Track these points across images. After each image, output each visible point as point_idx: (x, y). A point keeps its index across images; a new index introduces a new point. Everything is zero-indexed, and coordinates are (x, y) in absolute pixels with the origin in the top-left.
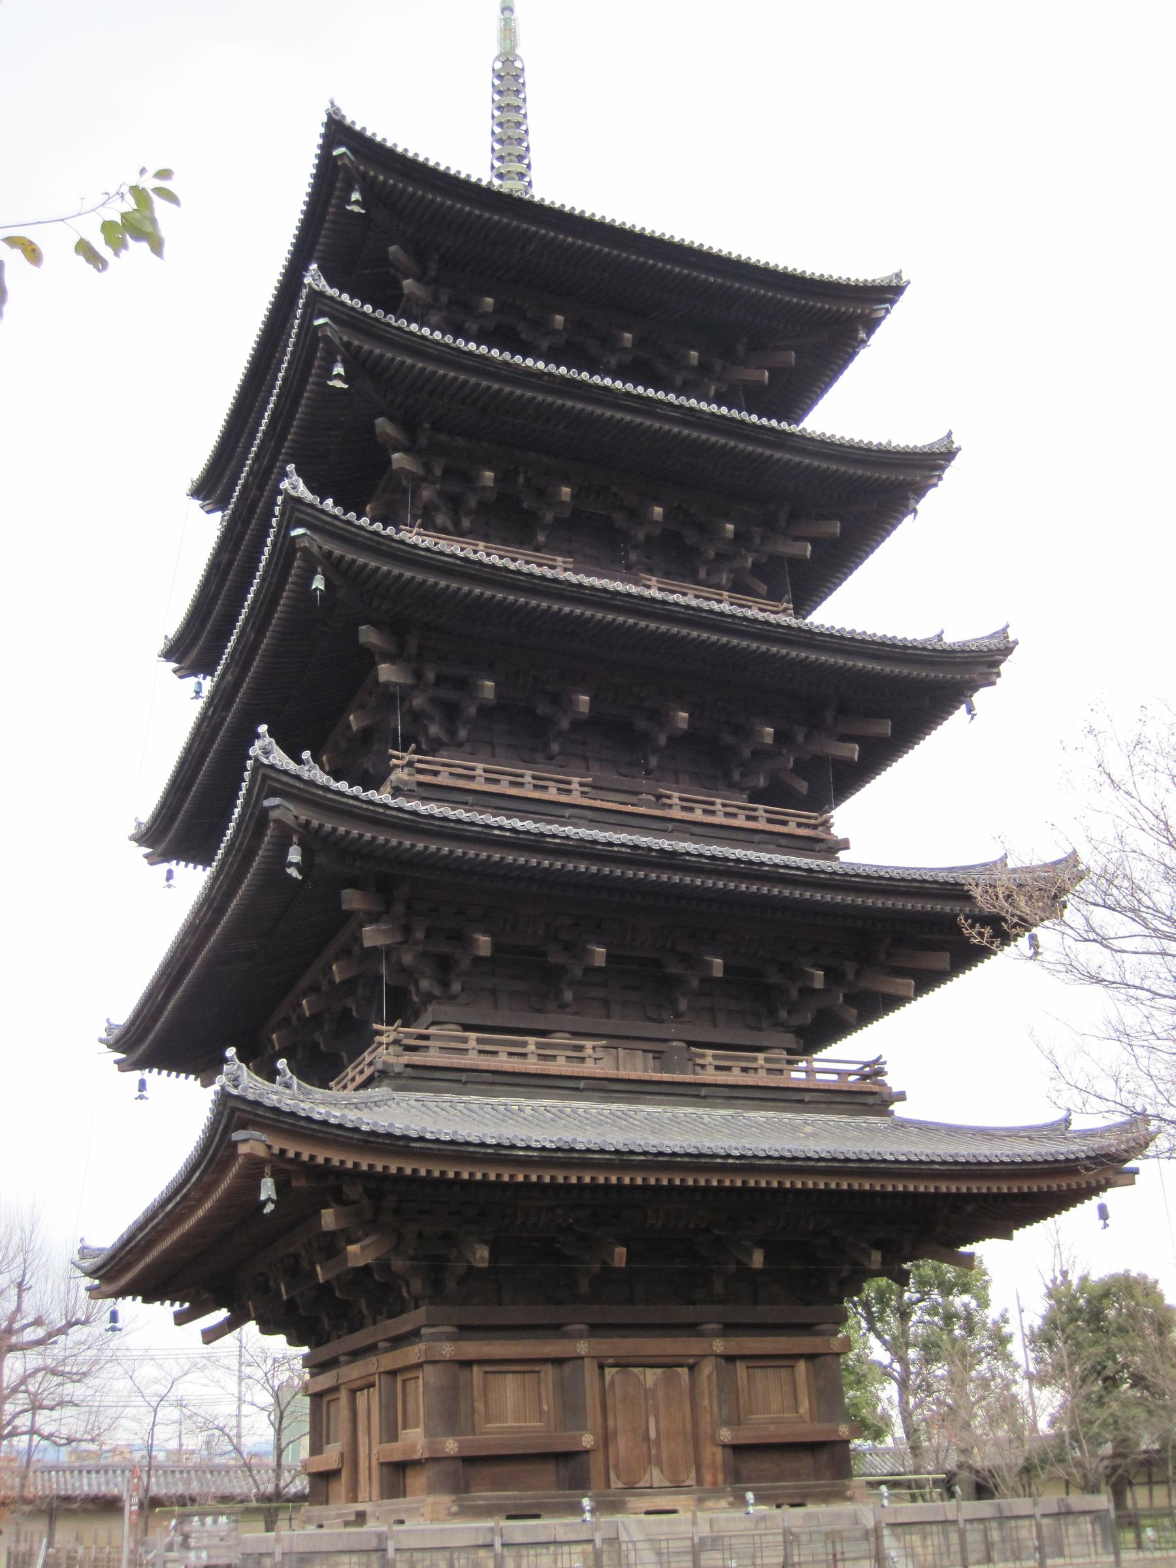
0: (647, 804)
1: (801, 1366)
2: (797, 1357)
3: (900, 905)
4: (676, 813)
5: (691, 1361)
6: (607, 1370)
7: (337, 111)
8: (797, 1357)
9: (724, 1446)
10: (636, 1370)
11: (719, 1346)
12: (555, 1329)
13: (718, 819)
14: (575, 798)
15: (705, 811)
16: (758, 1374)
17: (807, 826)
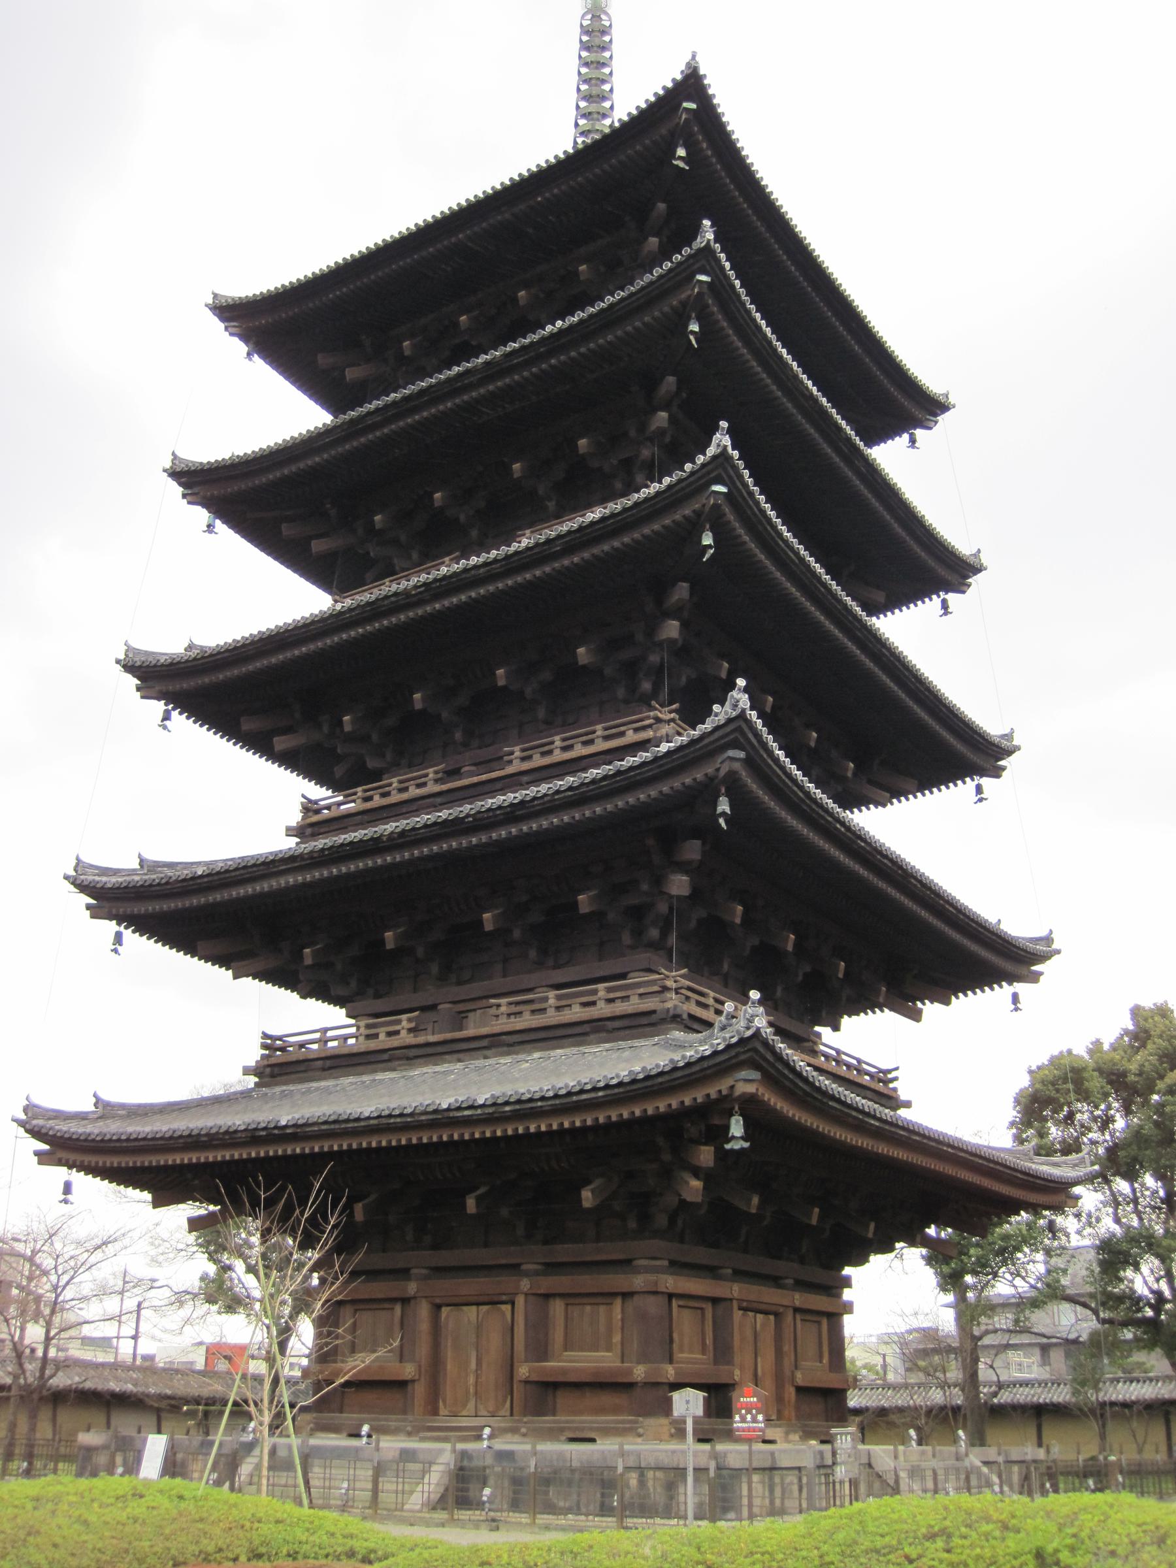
0: (472, 774)
1: (618, 1302)
2: (614, 1295)
3: (545, 824)
4: (516, 766)
5: (504, 1298)
6: (443, 1309)
7: (215, 296)
8: (614, 1295)
9: (526, 1382)
10: (465, 1308)
11: (525, 1284)
12: (403, 1273)
13: (558, 756)
14: (433, 788)
15: (543, 754)
16: (575, 1311)
17: (644, 728)
